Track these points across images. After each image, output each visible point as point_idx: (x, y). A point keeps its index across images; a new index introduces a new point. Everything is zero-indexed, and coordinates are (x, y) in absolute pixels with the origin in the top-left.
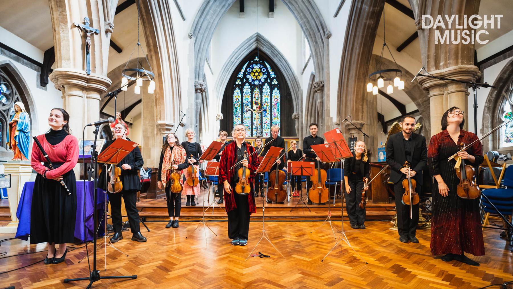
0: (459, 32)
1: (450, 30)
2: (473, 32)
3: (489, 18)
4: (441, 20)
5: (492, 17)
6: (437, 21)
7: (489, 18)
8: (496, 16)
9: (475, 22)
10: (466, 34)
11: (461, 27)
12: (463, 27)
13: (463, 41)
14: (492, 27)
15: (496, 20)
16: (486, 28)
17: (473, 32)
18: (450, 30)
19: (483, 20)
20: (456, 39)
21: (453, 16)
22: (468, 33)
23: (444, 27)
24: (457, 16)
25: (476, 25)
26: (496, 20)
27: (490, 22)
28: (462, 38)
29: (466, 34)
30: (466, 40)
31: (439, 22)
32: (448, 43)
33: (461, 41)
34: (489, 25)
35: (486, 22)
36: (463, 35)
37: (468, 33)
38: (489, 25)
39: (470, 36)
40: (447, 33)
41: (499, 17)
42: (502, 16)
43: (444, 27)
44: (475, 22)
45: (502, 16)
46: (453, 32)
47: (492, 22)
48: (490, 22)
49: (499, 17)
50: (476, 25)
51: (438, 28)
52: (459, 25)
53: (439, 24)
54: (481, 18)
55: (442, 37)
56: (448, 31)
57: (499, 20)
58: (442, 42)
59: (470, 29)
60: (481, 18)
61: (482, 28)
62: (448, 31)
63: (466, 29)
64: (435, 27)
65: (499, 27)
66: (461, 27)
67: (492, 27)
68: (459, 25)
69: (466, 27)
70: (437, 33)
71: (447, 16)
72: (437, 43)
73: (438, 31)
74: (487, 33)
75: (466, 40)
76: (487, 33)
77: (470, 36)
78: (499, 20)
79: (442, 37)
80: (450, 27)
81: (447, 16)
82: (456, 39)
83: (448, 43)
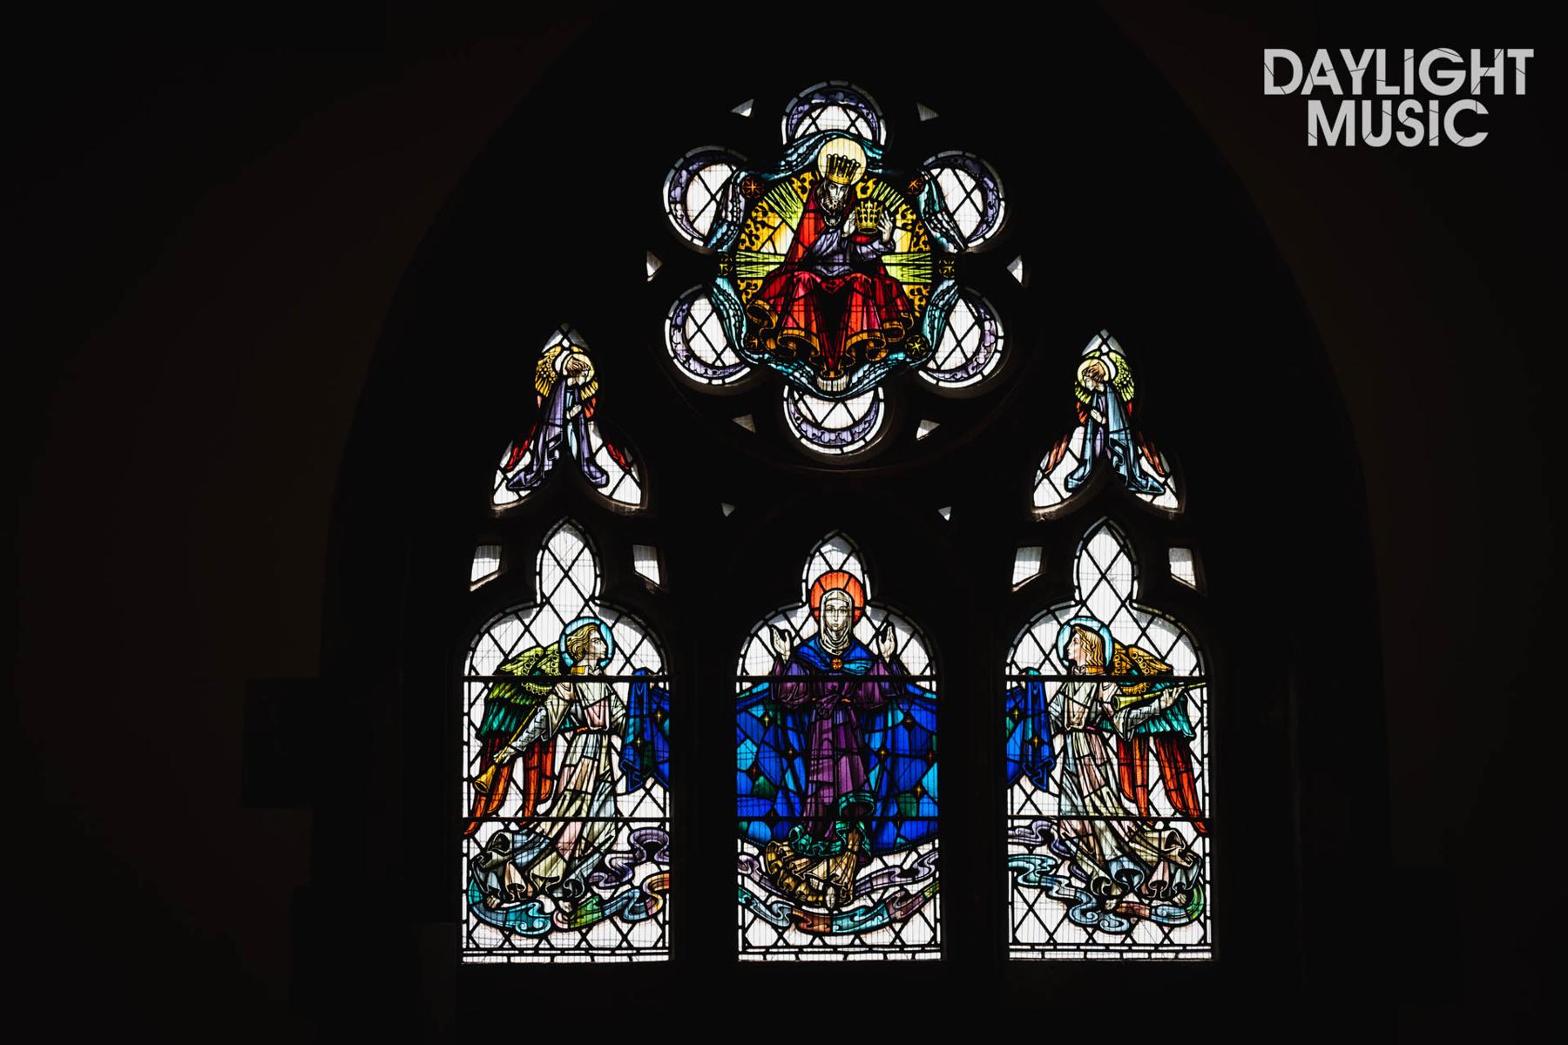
0: (1387, 106)
1: (1359, 100)
2: (1434, 105)
3: (1487, 61)
4: (1328, 66)
5: (1499, 55)
6: (1315, 69)
7: (1487, 61)
8: (1512, 53)
9: (1442, 74)
10: (1410, 112)
11: (1395, 90)
12: (1402, 90)
13: (1401, 136)
14: (1499, 89)
15: (1510, 64)
16: (1477, 92)
17: (1434, 105)
18: (1359, 100)
19: (1466, 66)
20: (1377, 131)
21: (1368, 53)
22: (1418, 108)
23: (1337, 90)
24: (1381, 53)
25: (1447, 82)
26: (1510, 64)
27: (1491, 72)
28: (1397, 125)
29: (1410, 112)
30: (1410, 133)
31: (1322, 72)
32: (1350, 141)
33: (1394, 136)
34: (1487, 82)
35: (1478, 72)
36: (1402, 116)
37: (1418, 108)
38: (1487, 82)
39: (1424, 118)
40: (1348, 108)
41: (1521, 55)
42: (1530, 53)
43: (1337, 90)
44: (1442, 74)
45: (1530, 53)
46: (1367, 105)
47: (1497, 72)
48: (1491, 72)
49: (1521, 55)
50: (1447, 82)
51: (1321, 93)
52: (1389, 83)
53: (1321, 81)
54: (1460, 60)
55: (1332, 126)
56: (1352, 103)
57: (1521, 65)
58: (1332, 139)
59: (1422, 95)
60: (1460, 60)
61: (1464, 92)
62: (1352, 103)
63: (1409, 97)
64: (1307, 91)
65: (1521, 89)
66: (1395, 90)
67: (1499, 89)
68: (1389, 83)
69: (1409, 89)
70: (1315, 109)
71: (1346, 54)
72: (1313, 142)
73: (1318, 103)
74: (1481, 110)
75: (1410, 133)
76: (1481, 110)
77: (1424, 118)
78: (1521, 65)
79: (1332, 126)
80: (1357, 89)
81: (1346, 54)
82: (1377, 131)
83: (1350, 141)
